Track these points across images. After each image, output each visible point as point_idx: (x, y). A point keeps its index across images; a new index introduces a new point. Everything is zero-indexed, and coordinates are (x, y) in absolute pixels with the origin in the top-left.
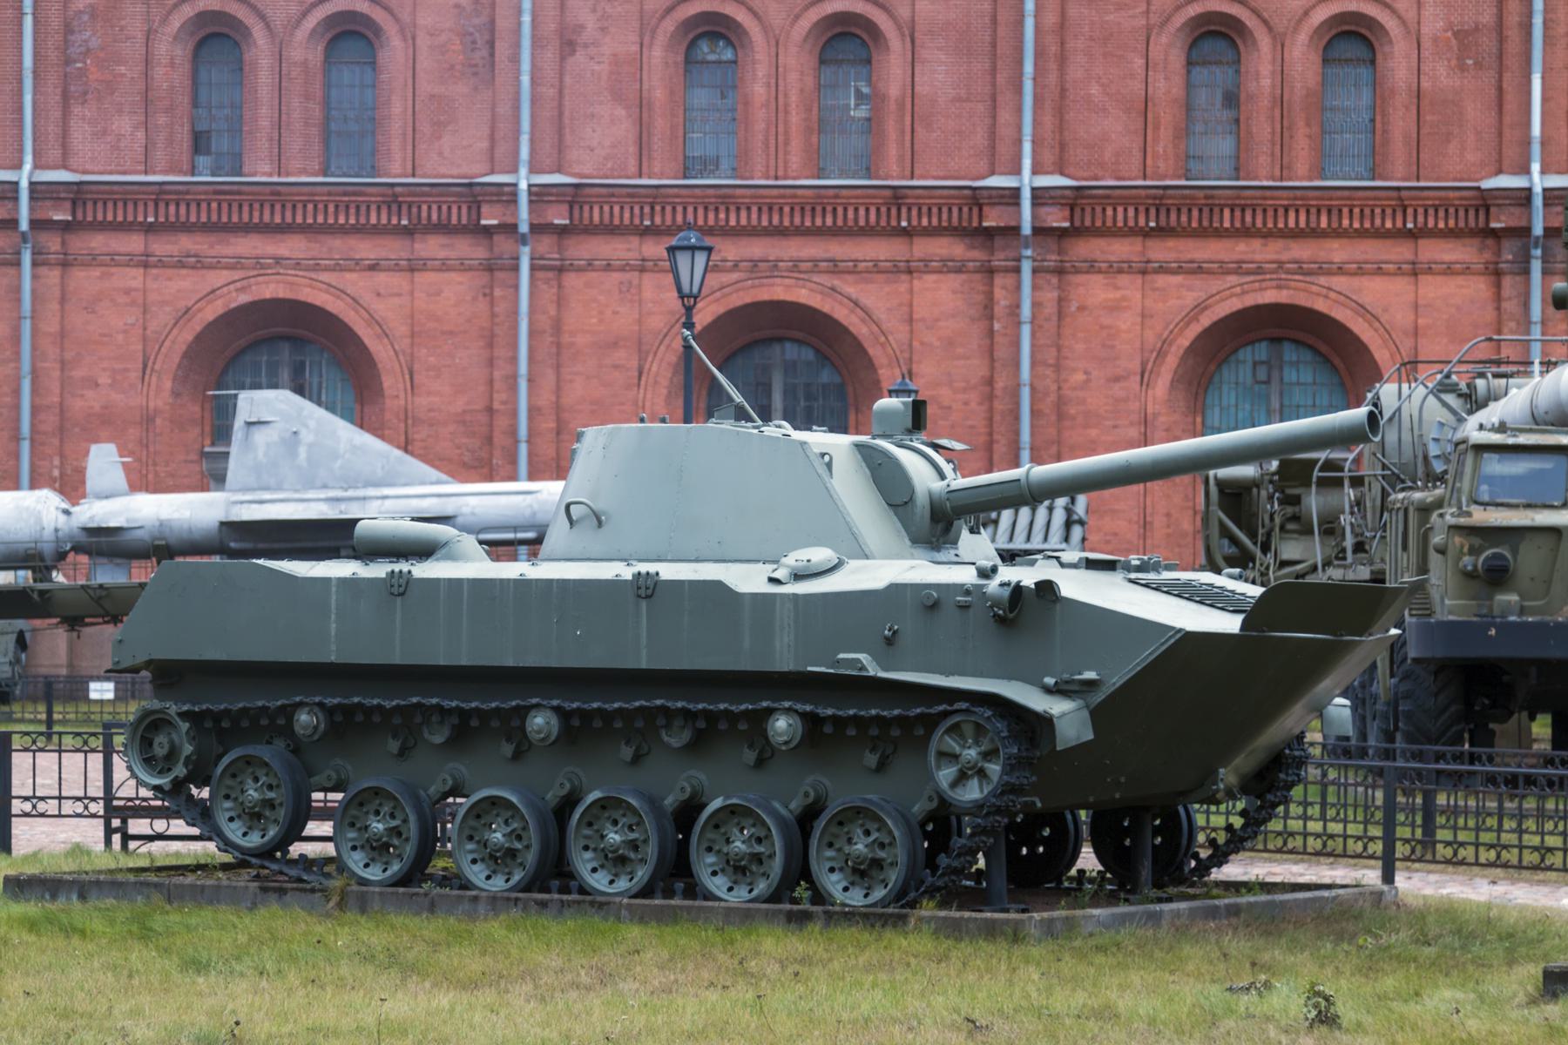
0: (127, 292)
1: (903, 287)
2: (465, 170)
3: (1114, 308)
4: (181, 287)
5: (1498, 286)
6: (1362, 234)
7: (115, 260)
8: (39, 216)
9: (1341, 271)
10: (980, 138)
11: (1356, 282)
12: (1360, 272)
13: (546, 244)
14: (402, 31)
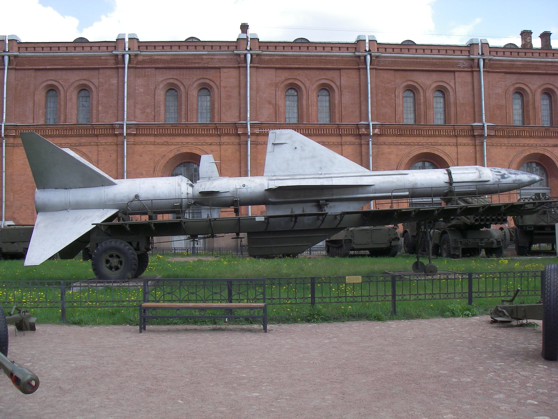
0: (150, 151)
1: (340, 149)
2: (233, 120)
3: (390, 153)
4: (163, 149)
5: (476, 148)
6: (445, 136)
7: (147, 143)
8: (129, 132)
9: (441, 145)
10: (357, 113)
11: (444, 147)
12: (445, 145)
13: (254, 138)
14: (217, 87)
